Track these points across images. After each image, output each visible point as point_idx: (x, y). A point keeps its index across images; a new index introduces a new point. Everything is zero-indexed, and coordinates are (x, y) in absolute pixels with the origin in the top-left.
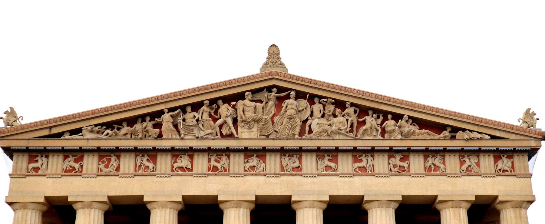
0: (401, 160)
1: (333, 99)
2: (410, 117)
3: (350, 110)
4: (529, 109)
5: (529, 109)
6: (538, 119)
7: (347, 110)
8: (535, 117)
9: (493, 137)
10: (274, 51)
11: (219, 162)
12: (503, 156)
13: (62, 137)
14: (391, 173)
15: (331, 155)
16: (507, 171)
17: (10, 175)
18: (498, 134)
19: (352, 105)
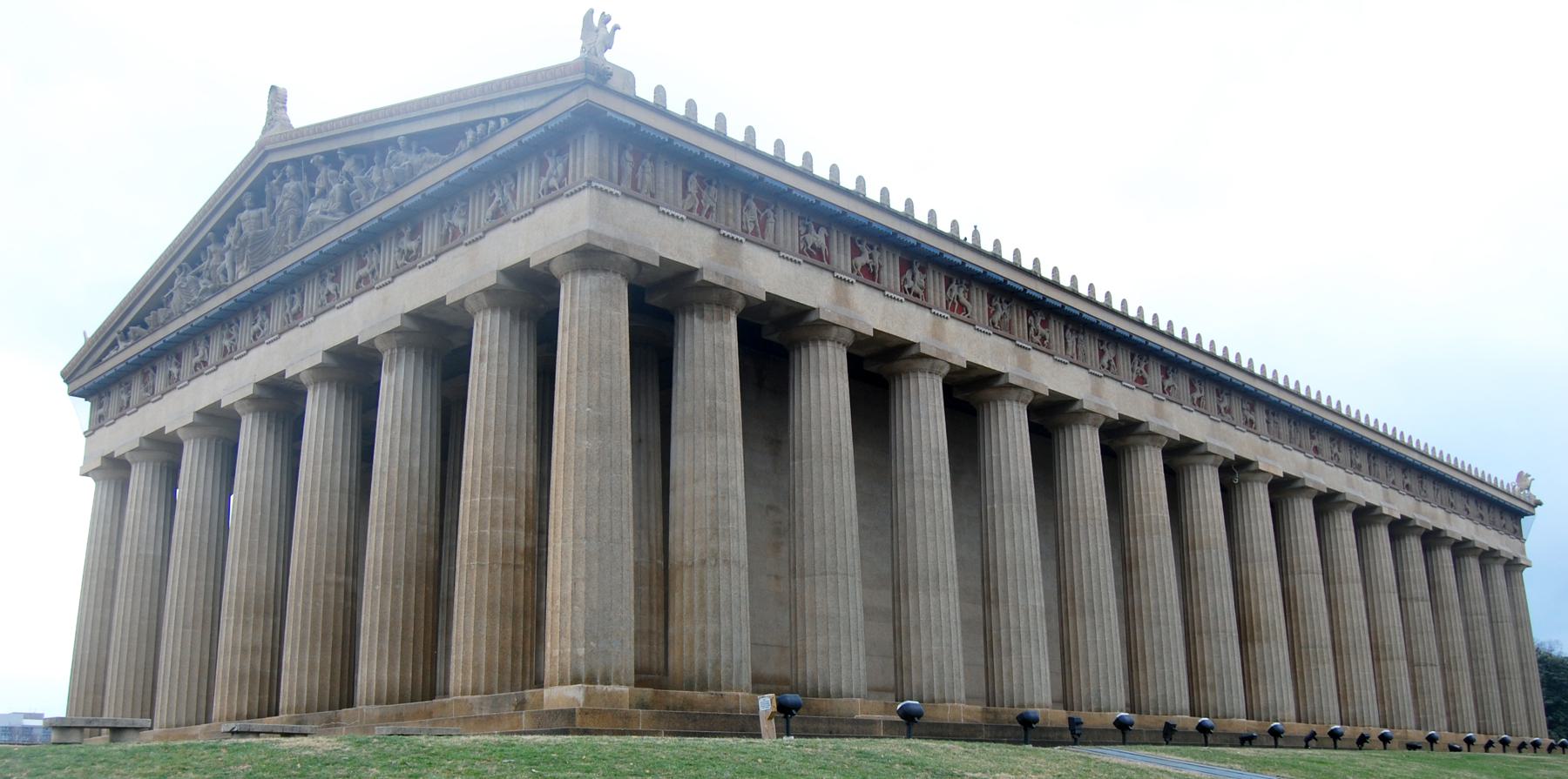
0: (412, 238)
1: (321, 154)
2: (410, 138)
3: (349, 165)
4: (591, 12)
5: (591, 12)
6: (616, 28)
7: (345, 168)
8: (609, 26)
9: (514, 118)
10: (277, 98)
11: (230, 336)
12: (550, 155)
13: (104, 359)
14: (401, 271)
15: (333, 268)
16: (554, 189)
17: (85, 433)
18: (519, 107)
19: (349, 151)
